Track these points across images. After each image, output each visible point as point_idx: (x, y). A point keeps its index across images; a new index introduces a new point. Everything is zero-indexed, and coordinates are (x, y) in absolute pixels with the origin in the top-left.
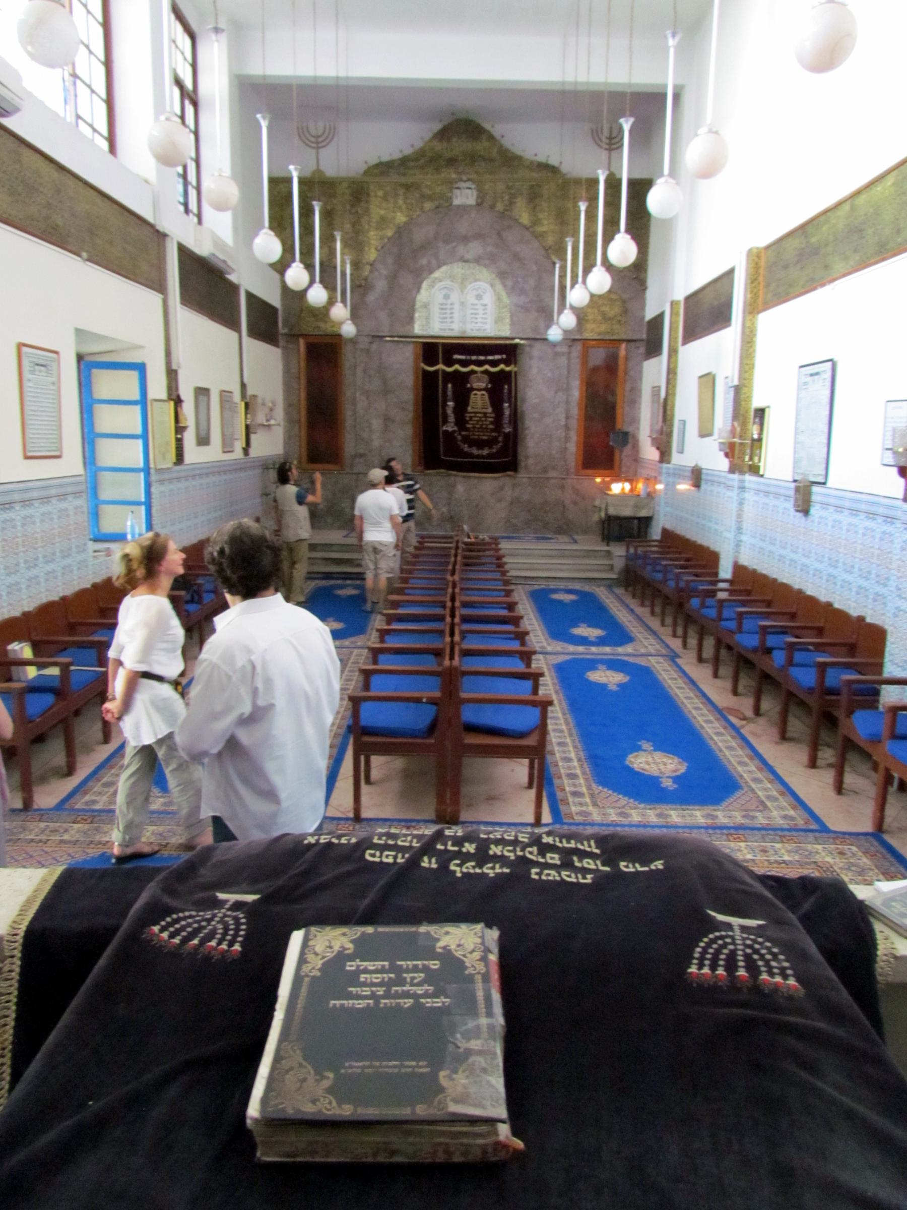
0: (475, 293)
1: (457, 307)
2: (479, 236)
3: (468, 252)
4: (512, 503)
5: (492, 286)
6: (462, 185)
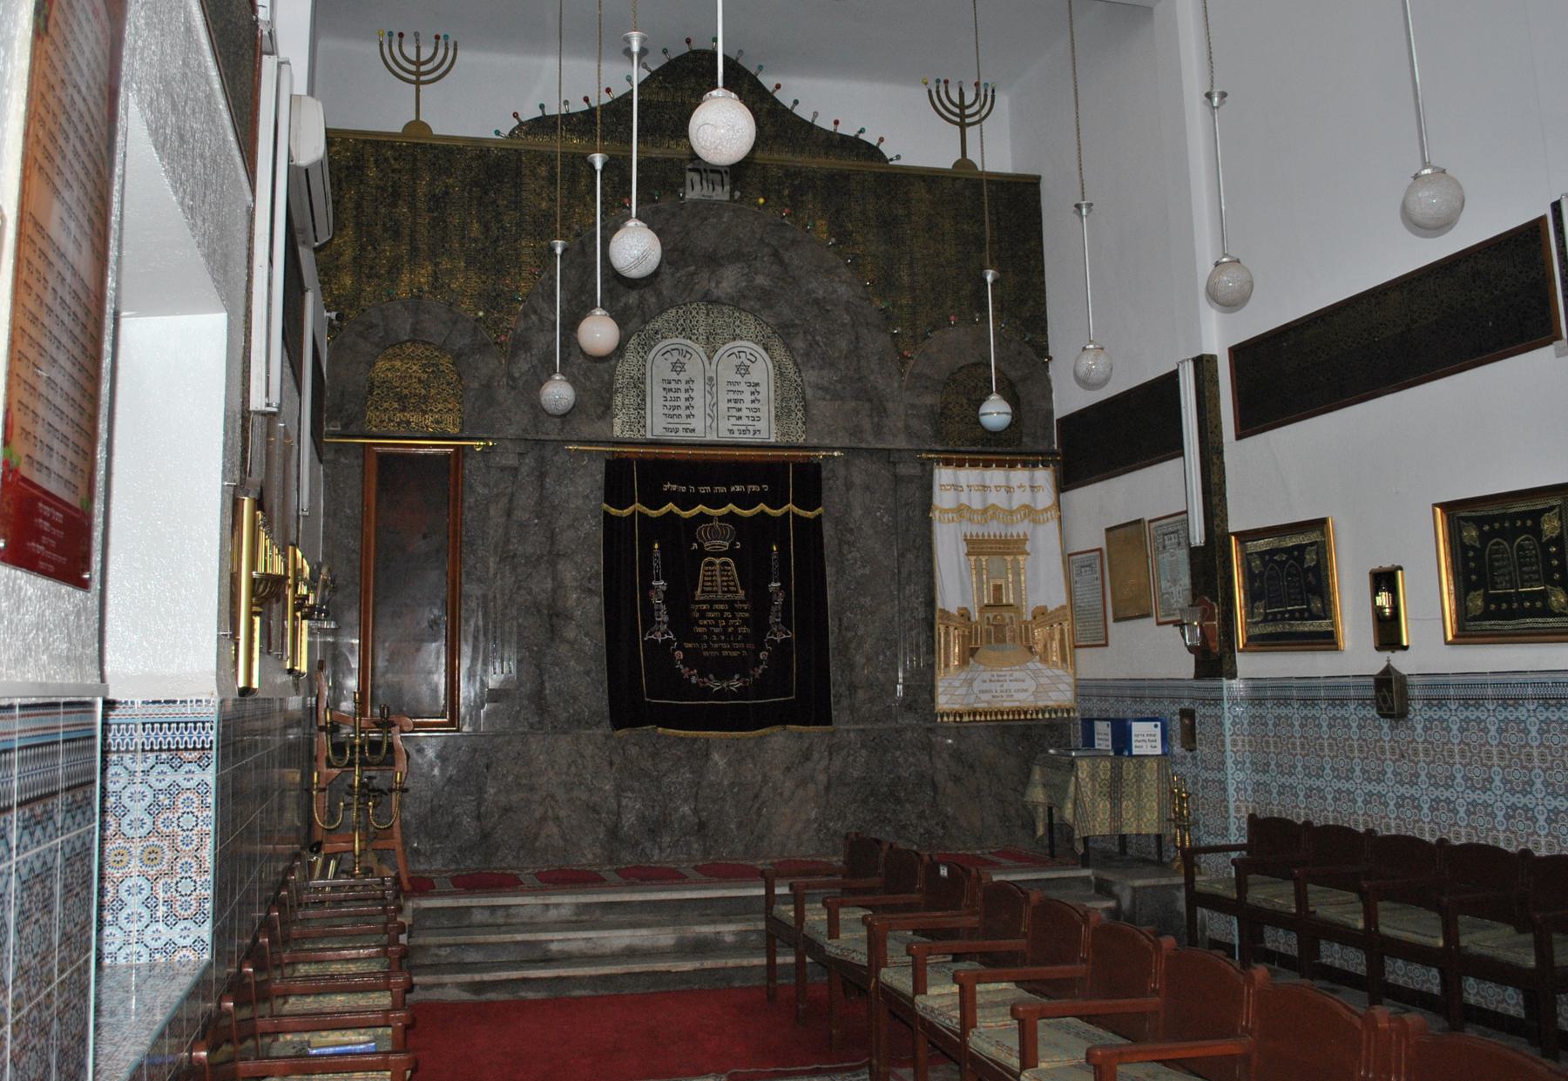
0: (735, 361)
1: (698, 386)
2: (738, 256)
3: (718, 283)
4: (828, 788)
5: (766, 349)
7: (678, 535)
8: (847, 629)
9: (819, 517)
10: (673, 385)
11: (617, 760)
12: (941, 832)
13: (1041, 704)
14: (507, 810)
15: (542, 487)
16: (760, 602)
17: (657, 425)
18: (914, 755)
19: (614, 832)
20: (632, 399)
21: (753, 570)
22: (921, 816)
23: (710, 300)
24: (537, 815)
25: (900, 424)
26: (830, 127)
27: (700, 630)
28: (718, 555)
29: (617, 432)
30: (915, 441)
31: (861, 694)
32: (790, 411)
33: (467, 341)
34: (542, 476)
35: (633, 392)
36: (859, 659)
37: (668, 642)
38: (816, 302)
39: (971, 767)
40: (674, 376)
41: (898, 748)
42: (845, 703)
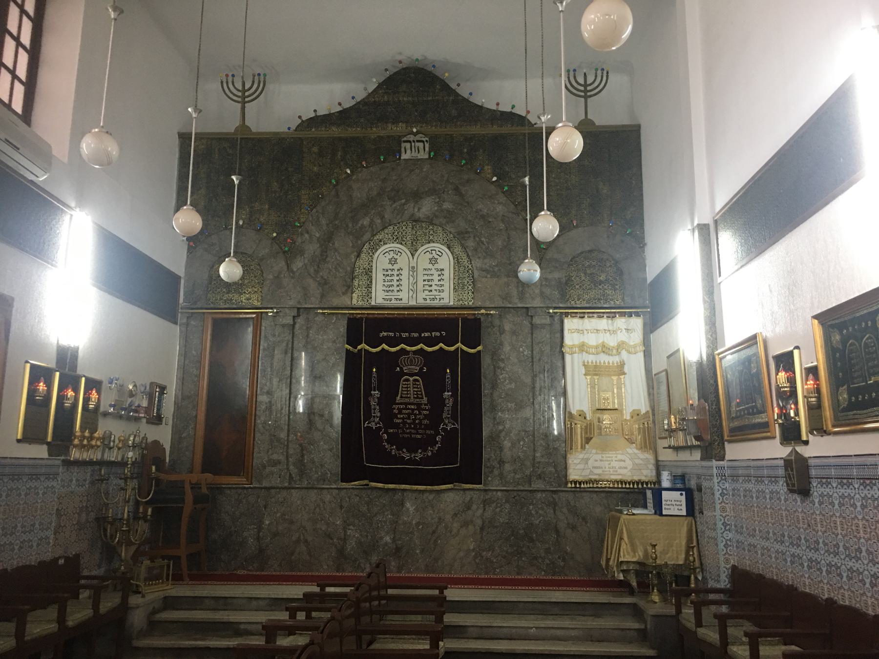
0: (429, 256)
1: (405, 273)
2: (433, 192)
3: (419, 209)
4: (482, 529)
5: (449, 248)
6: (411, 138)
7: (388, 362)
8: (498, 424)
9: (479, 352)
10: (390, 272)
11: (345, 505)
12: (562, 564)
13: (636, 478)
14: (275, 535)
15: (307, 336)
16: (437, 403)
17: (379, 297)
18: (542, 509)
19: (341, 552)
20: (364, 282)
22: (548, 551)
24: (294, 538)
25: (537, 291)
26: (494, 107)
27: (398, 421)
28: (412, 375)
29: (354, 301)
30: (548, 302)
31: (507, 467)
32: (464, 285)
33: (267, 251)
34: (308, 329)
35: (365, 278)
36: (507, 444)
37: (379, 429)
38: (483, 217)
39: (584, 519)
40: (390, 266)
41: (532, 504)
42: (496, 472)
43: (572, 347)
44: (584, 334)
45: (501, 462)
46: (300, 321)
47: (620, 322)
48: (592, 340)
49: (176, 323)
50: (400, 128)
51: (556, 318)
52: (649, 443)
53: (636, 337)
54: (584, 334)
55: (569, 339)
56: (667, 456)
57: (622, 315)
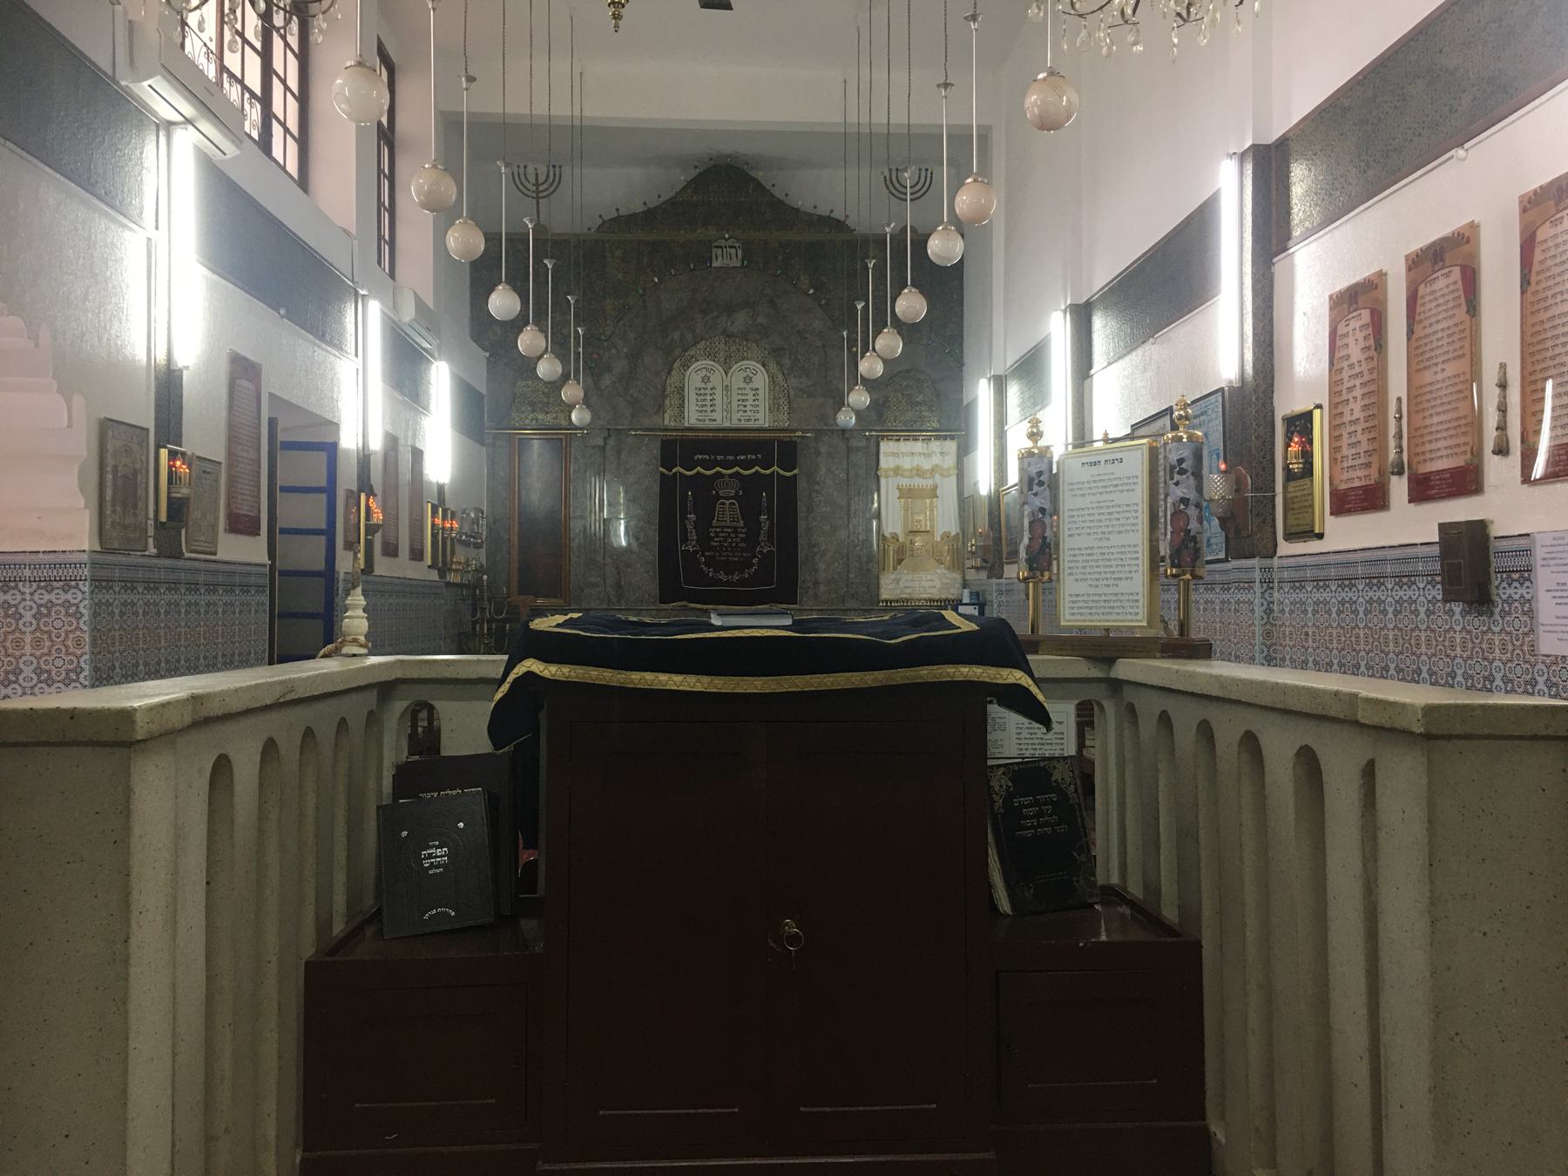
1: (719, 392)
6: (722, 243)
7: (703, 486)
17: (692, 418)
21: (749, 509)
23: (730, 336)
29: (666, 422)
31: (822, 588)
34: (619, 452)
36: (822, 566)
37: (696, 552)
42: (811, 593)
43: (886, 471)
44: (901, 458)
45: (816, 583)
46: (611, 442)
47: (935, 445)
48: (907, 463)
49: (482, 444)
50: (712, 232)
51: (873, 441)
52: (957, 564)
53: (950, 461)
54: (901, 458)
55: (886, 462)
56: (971, 575)
57: (938, 438)
